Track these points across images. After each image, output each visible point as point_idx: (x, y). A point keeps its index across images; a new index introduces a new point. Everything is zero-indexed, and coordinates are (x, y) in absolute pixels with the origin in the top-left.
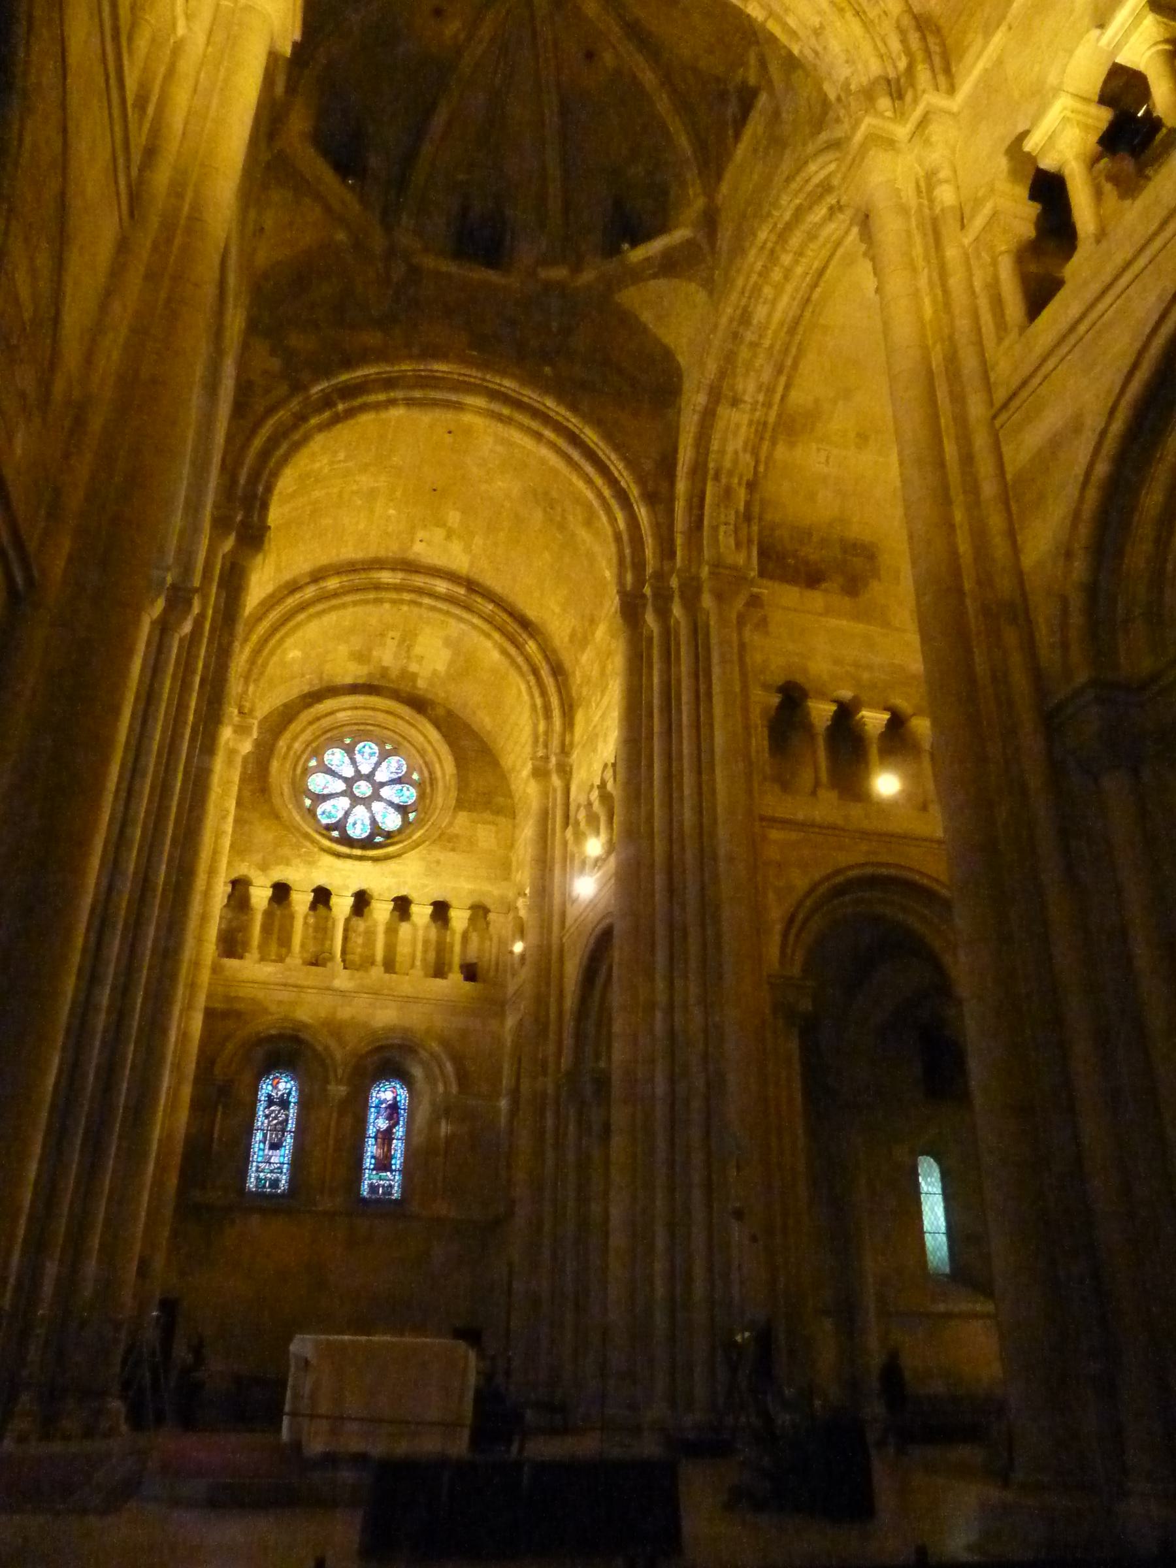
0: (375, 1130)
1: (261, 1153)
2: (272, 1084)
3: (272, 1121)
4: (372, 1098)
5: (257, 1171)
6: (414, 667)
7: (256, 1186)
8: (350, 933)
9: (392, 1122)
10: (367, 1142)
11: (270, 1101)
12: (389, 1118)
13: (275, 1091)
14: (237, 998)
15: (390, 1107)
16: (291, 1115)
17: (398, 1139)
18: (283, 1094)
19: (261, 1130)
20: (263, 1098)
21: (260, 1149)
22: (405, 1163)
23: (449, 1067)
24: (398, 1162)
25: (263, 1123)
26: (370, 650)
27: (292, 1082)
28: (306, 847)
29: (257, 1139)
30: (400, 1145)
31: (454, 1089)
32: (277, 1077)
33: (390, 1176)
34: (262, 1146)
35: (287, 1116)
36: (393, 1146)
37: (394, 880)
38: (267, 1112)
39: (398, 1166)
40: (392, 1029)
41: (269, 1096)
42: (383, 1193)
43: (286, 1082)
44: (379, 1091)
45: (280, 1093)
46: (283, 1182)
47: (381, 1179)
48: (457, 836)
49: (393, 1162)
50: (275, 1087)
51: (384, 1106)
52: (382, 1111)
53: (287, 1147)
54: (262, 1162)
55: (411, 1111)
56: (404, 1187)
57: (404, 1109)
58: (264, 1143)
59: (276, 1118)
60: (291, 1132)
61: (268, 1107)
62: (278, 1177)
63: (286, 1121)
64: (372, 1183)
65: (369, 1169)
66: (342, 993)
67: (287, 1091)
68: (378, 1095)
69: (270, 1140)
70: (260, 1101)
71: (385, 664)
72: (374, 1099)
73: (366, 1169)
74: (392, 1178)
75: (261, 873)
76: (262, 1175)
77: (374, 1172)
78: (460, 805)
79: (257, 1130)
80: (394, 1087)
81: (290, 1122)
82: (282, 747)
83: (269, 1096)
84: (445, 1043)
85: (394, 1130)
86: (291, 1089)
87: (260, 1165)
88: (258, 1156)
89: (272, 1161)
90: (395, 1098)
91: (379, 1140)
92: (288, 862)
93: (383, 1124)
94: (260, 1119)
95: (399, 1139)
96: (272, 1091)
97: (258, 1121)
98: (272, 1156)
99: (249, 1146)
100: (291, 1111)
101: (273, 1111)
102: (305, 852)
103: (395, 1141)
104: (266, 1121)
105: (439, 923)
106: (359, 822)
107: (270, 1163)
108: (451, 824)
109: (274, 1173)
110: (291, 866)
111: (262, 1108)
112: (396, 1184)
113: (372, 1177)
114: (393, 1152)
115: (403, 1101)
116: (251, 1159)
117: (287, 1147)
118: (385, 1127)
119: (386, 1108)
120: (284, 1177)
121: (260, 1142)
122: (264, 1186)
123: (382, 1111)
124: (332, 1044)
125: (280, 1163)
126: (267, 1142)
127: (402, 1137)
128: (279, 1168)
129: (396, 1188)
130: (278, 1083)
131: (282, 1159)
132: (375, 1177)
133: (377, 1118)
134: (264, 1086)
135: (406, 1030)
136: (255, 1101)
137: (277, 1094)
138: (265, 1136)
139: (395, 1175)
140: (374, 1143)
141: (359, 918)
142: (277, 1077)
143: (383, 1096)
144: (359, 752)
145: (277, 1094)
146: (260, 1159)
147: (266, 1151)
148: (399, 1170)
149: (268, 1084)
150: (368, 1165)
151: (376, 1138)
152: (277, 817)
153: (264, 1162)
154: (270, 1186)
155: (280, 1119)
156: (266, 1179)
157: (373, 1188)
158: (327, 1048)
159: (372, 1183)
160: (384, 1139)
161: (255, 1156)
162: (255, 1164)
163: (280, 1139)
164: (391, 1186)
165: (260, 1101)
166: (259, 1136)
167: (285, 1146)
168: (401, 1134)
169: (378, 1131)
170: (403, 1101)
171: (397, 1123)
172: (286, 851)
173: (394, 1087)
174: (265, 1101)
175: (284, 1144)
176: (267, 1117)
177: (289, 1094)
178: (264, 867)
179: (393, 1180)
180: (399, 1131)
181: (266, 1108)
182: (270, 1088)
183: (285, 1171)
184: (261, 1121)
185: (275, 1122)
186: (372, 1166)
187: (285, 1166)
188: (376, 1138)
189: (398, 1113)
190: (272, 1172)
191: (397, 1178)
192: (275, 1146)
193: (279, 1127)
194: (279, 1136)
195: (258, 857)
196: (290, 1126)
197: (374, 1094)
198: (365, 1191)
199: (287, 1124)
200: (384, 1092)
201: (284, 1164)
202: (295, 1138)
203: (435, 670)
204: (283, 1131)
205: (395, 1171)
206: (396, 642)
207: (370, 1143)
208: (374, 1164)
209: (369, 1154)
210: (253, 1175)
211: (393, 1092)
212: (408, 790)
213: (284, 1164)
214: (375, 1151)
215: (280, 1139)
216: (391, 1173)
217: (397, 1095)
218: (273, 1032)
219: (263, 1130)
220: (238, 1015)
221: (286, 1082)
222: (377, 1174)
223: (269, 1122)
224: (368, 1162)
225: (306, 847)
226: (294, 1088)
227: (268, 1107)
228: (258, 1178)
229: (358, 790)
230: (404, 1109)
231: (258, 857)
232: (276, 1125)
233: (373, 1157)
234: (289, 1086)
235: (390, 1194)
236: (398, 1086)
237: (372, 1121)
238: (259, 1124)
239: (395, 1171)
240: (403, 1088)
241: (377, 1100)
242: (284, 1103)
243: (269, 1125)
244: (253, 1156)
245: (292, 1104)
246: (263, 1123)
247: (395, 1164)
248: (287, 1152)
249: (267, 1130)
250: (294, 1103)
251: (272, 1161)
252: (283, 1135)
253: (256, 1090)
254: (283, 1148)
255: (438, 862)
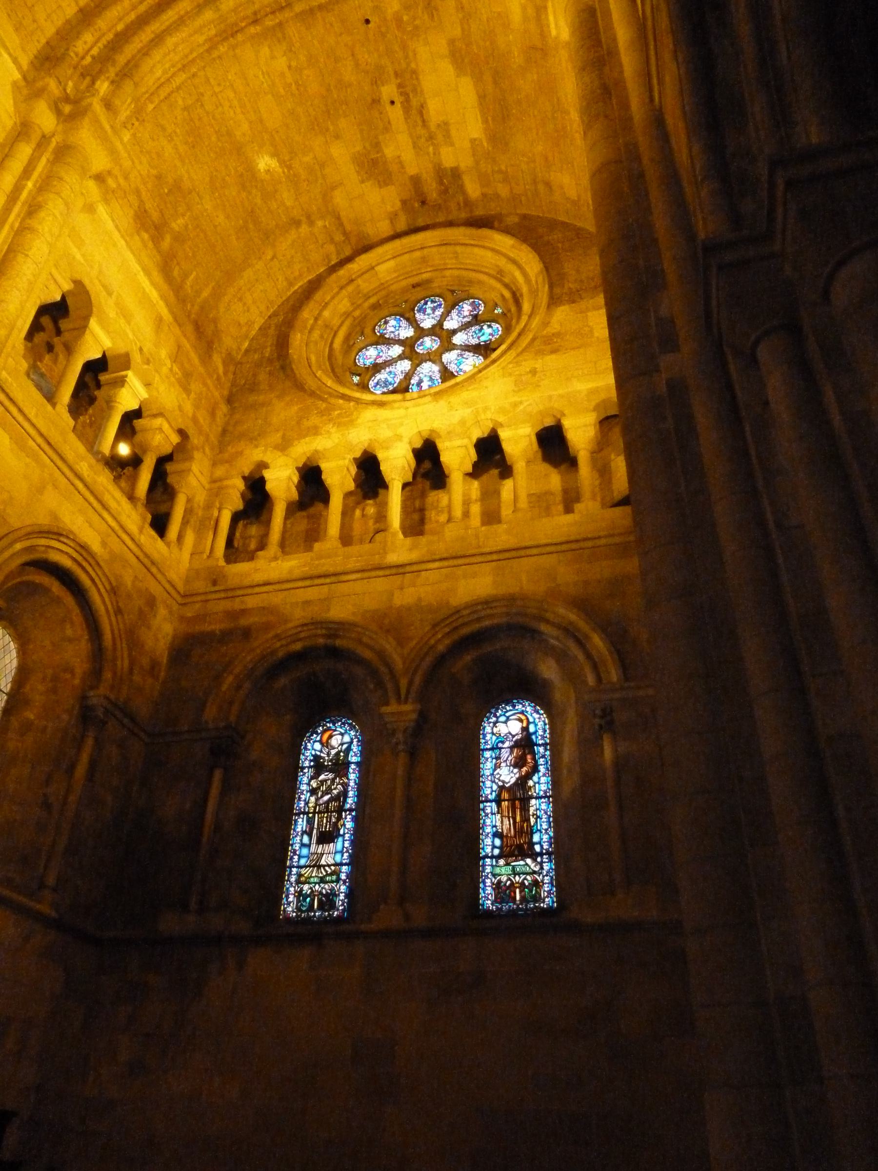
0: (495, 787)
1: (305, 851)
2: (321, 742)
3: (322, 796)
4: (485, 736)
5: (298, 882)
6: (449, 158)
7: (299, 909)
8: (427, 513)
9: (524, 769)
10: (483, 810)
11: (319, 766)
12: (519, 763)
13: (326, 750)
14: (244, 612)
15: (517, 745)
16: (352, 783)
17: (538, 798)
18: (338, 754)
19: (304, 813)
20: (307, 764)
21: (303, 845)
22: (556, 840)
23: (598, 642)
24: (545, 838)
25: (307, 803)
26: (377, 146)
27: (353, 733)
28: (341, 408)
29: (299, 829)
30: (544, 806)
31: (614, 675)
32: (329, 729)
33: (532, 866)
34: (306, 839)
35: (345, 786)
36: (532, 810)
37: (469, 411)
38: (314, 784)
39: (546, 846)
40: (488, 602)
41: (316, 758)
42: (523, 899)
43: (342, 734)
44: (495, 723)
45: (333, 752)
46: (342, 897)
47: (515, 874)
48: (558, 335)
49: (536, 838)
50: (326, 744)
51: (507, 744)
52: (505, 754)
53: (347, 837)
54: (306, 867)
55: (554, 745)
56: (561, 883)
57: (545, 745)
58: (310, 835)
59: (328, 791)
60: (351, 810)
61: (315, 776)
62: (332, 889)
63: (344, 794)
64: (500, 882)
65: (492, 857)
66: (399, 569)
67: (345, 746)
68: (495, 730)
69: (318, 828)
70: (303, 768)
71: (412, 171)
72: (488, 737)
73: (486, 856)
74: (537, 869)
75: (280, 453)
76: (306, 887)
77: (502, 862)
78: (554, 301)
79: (298, 814)
80: (522, 713)
81: (351, 794)
82: (307, 319)
83: (316, 758)
84: (581, 604)
85: (531, 783)
86: (351, 742)
87: (303, 871)
88: (300, 857)
89: (323, 862)
90: (525, 729)
91: (505, 804)
92: (315, 431)
93: (508, 775)
94: (303, 797)
95: (541, 797)
96: (321, 751)
97: (300, 798)
98: (322, 854)
99: (284, 843)
100: (352, 776)
101: (322, 782)
102: (338, 414)
103: (533, 802)
104: (313, 799)
105: (563, 467)
106: (426, 380)
107: (319, 867)
108: (546, 324)
109: (326, 882)
110: (321, 434)
111: (305, 780)
112: (547, 880)
113: (497, 870)
114: (532, 820)
115: (540, 732)
116: (288, 864)
117: (347, 837)
118: (513, 781)
119: (511, 748)
120: (343, 888)
121: (304, 832)
122: (311, 907)
123: (505, 754)
124: (389, 645)
125: (336, 865)
126: (315, 831)
127: (545, 792)
128: (333, 873)
129: (546, 888)
130: (331, 737)
131: (338, 858)
132: (503, 870)
133: (497, 766)
134: (309, 746)
135: (511, 599)
136: (296, 768)
137: (328, 754)
138: (310, 822)
139: (541, 863)
140: (495, 809)
141: (440, 491)
142: (329, 729)
143: (502, 729)
144: (419, 311)
145: (328, 754)
146: (303, 862)
147: (313, 847)
148: (548, 853)
149: (315, 742)
150: (488, 850)
151: (498, 801)
152: (300, 387)
153: (310, 866)
154: (321, 906)
155: (335, 792)
156: (312, 894)
157: (503, 892)
158: (381, 655)
159: (500, 882)
160: (512, 800)
161: (296, 857)
162: (294, 870)
163: (336, 824)
164: (536, 883)
165: (303, 768)
166: (301, 824)
167: (343, 836)
168: (544, 787)
169: (502, 788)
170: (540, 732)
171: (535, 769)
172: (314, 420)
173: (522, 713)
174: (310, 767)
175: (342, 832)
176: (313, 792)
177: (349, 749)
178: (283, 447)
179: (539, 874)
180: (541, 783)
181: (312, 778)
182: (318, 746)
183: (343, 876)
184: (305, 799)
185: (326, 798)
186: (496, 852)
187: (345, 869)
188: (498, 801)
189: (533, 754)
190: (322, 880)
191: (546, 867)
192: (326, 838)
193: (333, 805)
194: (334, 820)
195: (276, 438)
196: (350, 801)
197: (488, 729)
198: (487, 898)
199: (345, 801)
200: (505, 722)
201: (341, 864)
202: (355, 820)
203: (473, 141)
204: (340, 810)
205: (541, 854)
206: (398, 105)
207: (488, 810)
208: (501, 848)
209: (488, 830)
210: (292, 889)
211: (521, 720)
212: (490, 326)
213: (341, 864)
214: (498, 824)
215: (336, 824)
216: (535, 860)
217: (529, 723)
218: (298, 646)
219: (308, 813)
220: (247, 633)
221: (342, 734)
222: (507, 864)
223: (317, 800)
224: (489, 845)
225: (341, 408)
226: (355, 743)
227: (315, 776)
228: (300, 894)
229: (421, 348)
230: (545, 745)
231: (276, 438)
232: (328, 802)
233: (496, 835)
234: (347, 739)
235: (537, 898)
236: (529, 709)
237: (487, 773)
238: (302, 804)
239: (541, 854)
240: (538, 712)
241: (494, 738)
242: (340, 767)
243: (316, 804)
244: (292, 858)
245: (353, 766)
246: (307, 803)
247: (540, 843)
248: (347, 844)
249: (314, 813)
250: (357, 763)
251: (323, 862)
252: (339, 818)
253: (296, 751)
254: (340, 839)
255: (534, 372)
